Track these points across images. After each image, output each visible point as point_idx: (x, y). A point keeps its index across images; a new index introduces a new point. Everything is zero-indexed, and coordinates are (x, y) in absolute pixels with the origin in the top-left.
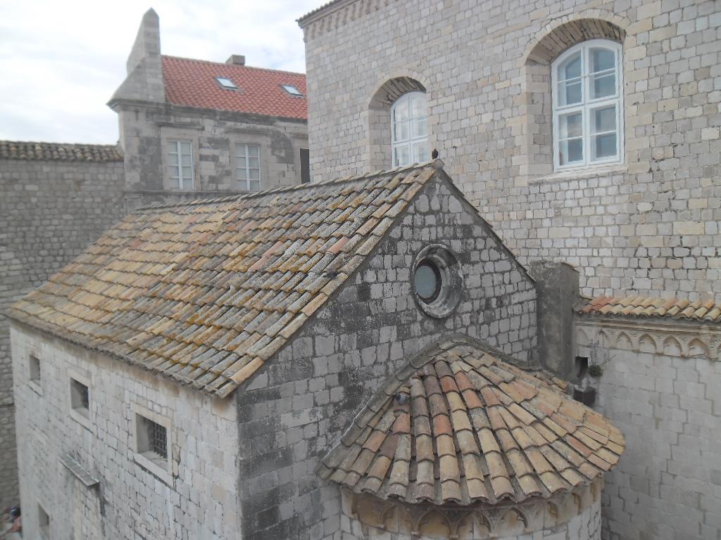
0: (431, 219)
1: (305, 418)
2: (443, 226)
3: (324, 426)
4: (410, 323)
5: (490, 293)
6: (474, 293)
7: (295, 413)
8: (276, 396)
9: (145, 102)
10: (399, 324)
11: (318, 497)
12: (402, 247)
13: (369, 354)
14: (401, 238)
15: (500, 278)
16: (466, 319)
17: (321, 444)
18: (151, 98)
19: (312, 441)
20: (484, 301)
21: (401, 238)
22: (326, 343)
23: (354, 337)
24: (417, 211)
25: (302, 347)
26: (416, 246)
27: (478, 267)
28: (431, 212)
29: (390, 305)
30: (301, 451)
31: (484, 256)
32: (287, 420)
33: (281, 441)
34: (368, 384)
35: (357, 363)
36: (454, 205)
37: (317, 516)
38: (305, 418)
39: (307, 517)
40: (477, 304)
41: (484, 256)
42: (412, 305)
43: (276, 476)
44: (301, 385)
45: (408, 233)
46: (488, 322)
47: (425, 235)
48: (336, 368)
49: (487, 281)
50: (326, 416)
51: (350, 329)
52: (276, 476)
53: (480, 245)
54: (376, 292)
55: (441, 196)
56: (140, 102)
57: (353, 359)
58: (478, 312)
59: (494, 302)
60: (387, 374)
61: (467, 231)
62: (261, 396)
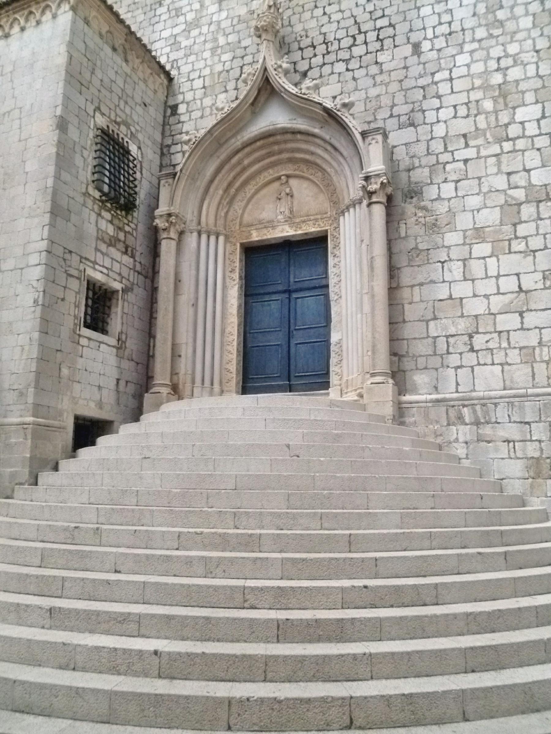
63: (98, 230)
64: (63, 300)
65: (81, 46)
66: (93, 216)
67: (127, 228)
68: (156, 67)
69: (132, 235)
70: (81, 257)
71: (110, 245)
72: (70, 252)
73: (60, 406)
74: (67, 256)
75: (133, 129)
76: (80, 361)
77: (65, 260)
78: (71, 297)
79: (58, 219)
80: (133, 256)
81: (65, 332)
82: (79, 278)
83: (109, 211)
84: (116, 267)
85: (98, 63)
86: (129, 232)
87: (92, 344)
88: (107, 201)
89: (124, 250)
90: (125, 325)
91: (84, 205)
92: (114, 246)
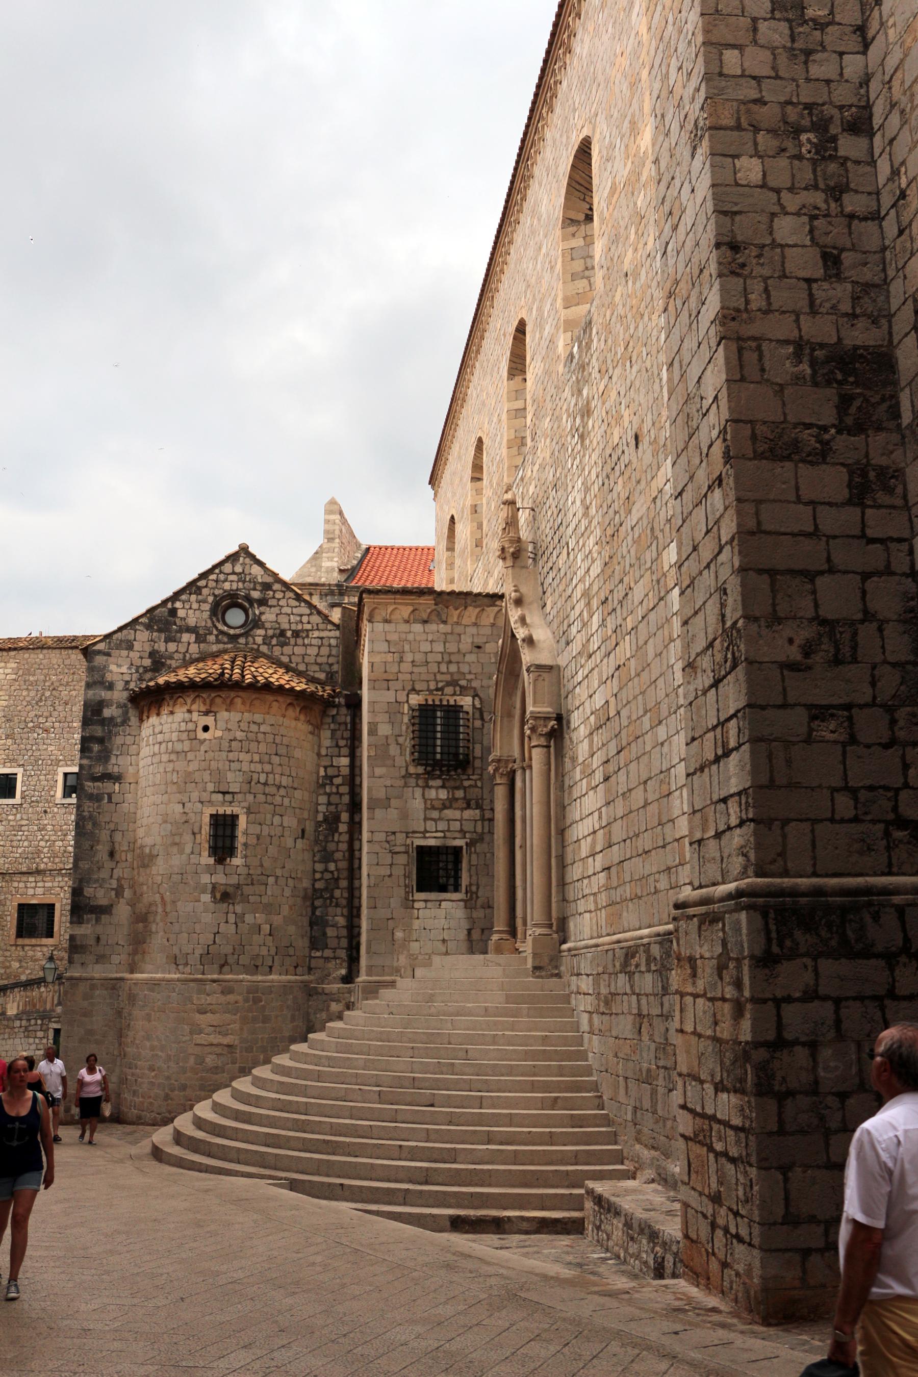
0: (234, 578)
1: (124, 669)
2: (244, 582)
3: (135, 676)
4: (206, 635)
5: (285, 626)
6: (267, 625)
7: (119, 666)
8: (109, 655)
9: (317, 585)
10: (197, 634)
11: (127, 712)
12: (205, 591)
13: (172, 647)
14: (206, 586)
15: (298, 618)
16: (259, 640)
17: (132, 685)
18: (323, 580)
19: (127, 682)
20: (278, 632)
21: (206, 586)
22: (143, 635)
23: (163, 636)
24: (221, 572)
25: (128, 634)
26: (217, 592)
27: (277, 610)
28: (234, 573)
29: (192, 622)
30: (120, 685)
31: (282, 603)
32: (113, 667)
33: (108, 677)
34: (169, 662)
35: (163, 649)
36: (256, 570)
37: (125, 721)
38: (124, 669)
39: (119, 720)
40: (270, 632)
41: (282, 603)
42: (209, 624)
43: (105, 694)
44: (124, 653)
45: (212, 584)
46: (282, 645)
47: (227, 586)
48: (148, 649)
49: (283, 620)
50: (137, 671)
51: (160, 631)
52: (105, 694)
53: (279, 595)
54: (181, 613)
55: (244, 564)
56: (311, 584)
57: (161, 646)
58: (272, 637)
59: (289, 634)
60: (184, 659)
61: (267, 587)
62: (99, 652)
63: (425, 801)
64: (390, 876)
65: (384, 647)
66: (418, 792)
67: (466, 783)
68: (486, 600)
69: (476, 786)
70: (407, 833)
71: (445, 807)
72: (394, 833)
73: (395, 964)
74: (392, 837)
75: (463, 683)
76: (416, 922)
77: (388, 842)
78: (399, 871)
79: (377, 811)
80: (479, 806)
81: (395, 902)
82: (406, 852)
83: (439, 777)
84: (456, 826)
85: (407, 648)
86: (470, 786)
87: (429, 905)
88: (433, 770)
89: (465, 805)
90: (474, 878)
91: (406, 785)
92: (450, 807)
